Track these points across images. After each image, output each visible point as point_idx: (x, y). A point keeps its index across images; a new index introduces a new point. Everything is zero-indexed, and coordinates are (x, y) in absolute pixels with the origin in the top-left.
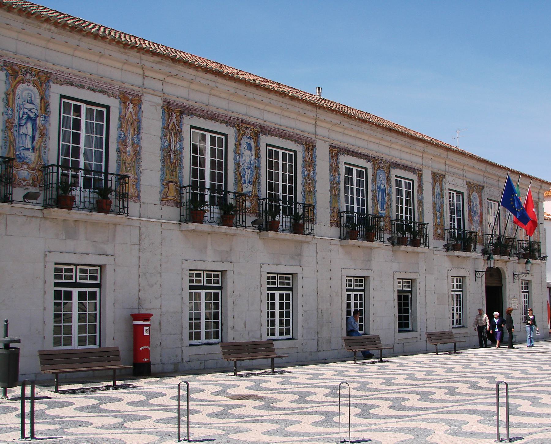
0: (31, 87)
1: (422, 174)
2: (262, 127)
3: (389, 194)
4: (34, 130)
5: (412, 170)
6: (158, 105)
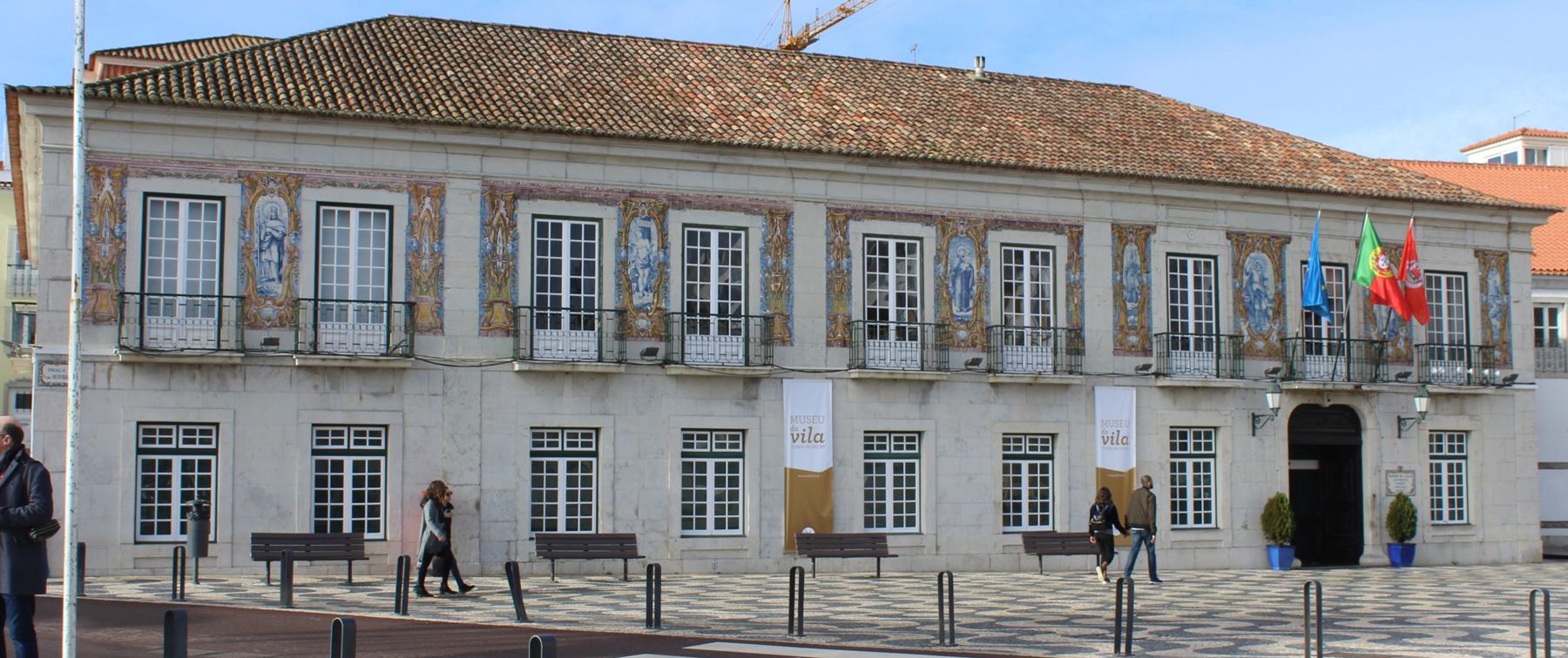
0: (276, 198)
1: (1081, 233)
3: (984, 280)
4: (280, 253)
6: (474, 192)
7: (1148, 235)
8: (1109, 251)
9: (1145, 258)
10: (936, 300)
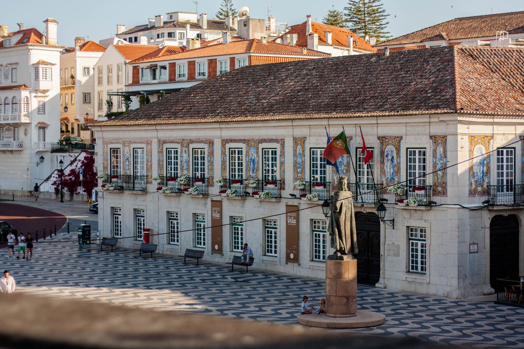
1: (284, 142)
2: (190, 140)
5: (276, 141)
7: (304, 141)
8: (292, 148)
9: (303, 151)
10: (246, 170)
